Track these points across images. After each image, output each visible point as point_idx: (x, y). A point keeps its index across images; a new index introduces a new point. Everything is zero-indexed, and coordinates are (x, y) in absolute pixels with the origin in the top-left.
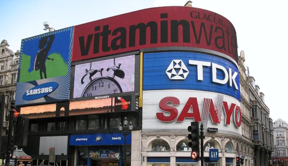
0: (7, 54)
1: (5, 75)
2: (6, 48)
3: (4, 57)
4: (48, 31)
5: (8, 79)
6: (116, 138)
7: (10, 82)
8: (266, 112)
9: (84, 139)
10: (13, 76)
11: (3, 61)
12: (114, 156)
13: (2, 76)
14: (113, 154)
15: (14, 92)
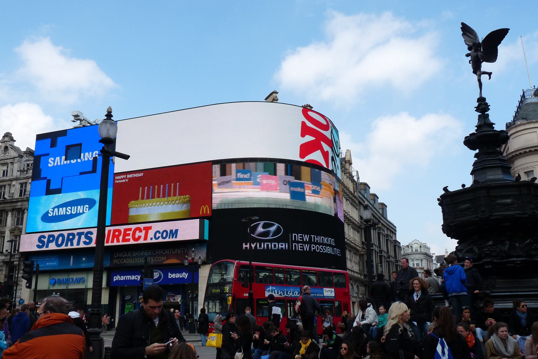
0: (12, 153)
1: (10, 185)
2: (11, 145)
3: (8, 157)
4: (77, 124)
5: (15, 190)
6: (178, 276)
7: (17, 196)
8: (391, 231)
9: (133, 278)
10: (22, 187)
11: (6, 164)
12: (174, 300)
13: (5, 186)
14: (173, 296)
15: (25, 209)
